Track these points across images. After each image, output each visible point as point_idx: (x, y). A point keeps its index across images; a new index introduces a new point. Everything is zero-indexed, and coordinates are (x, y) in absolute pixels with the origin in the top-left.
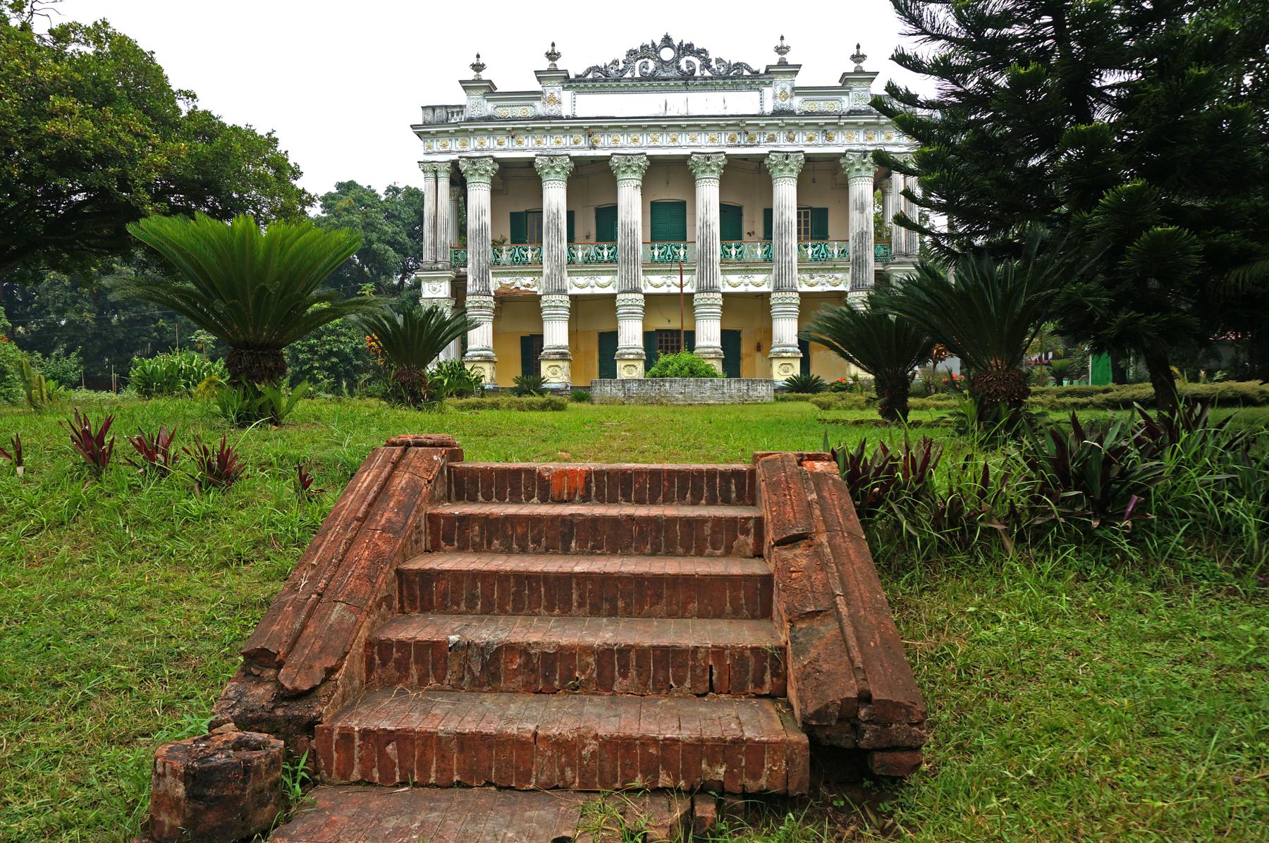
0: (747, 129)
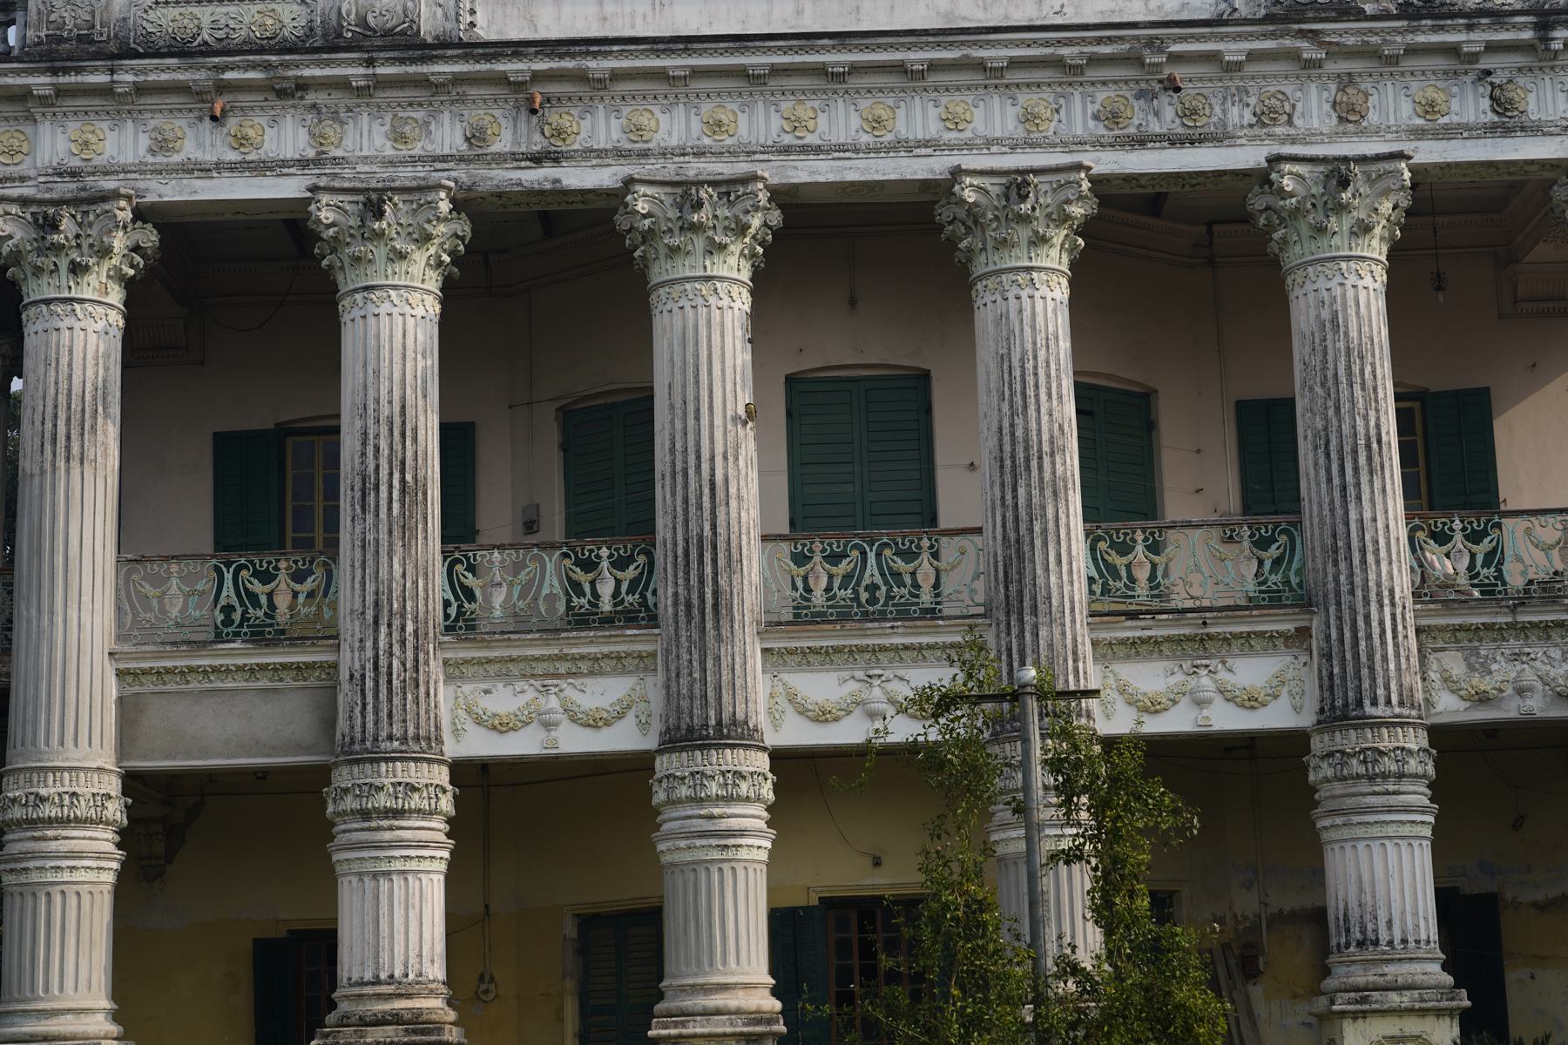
0: (1179, 72)
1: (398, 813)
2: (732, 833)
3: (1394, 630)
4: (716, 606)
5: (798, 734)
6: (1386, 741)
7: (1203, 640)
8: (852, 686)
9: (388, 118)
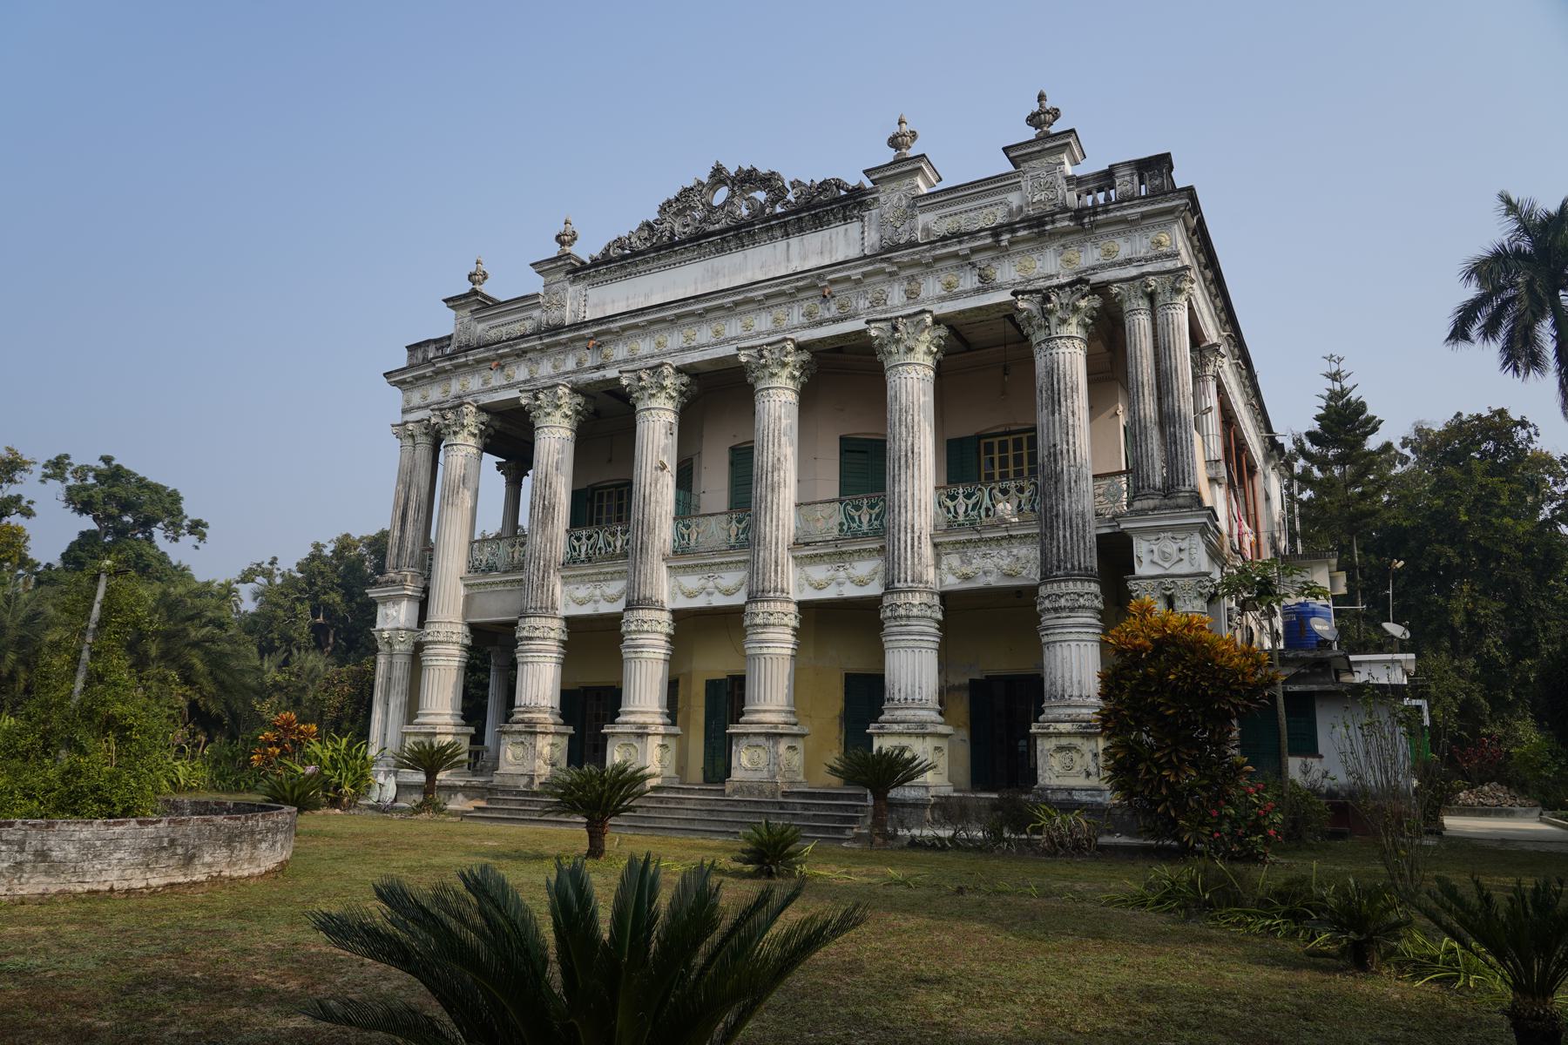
1: (531, 638)
2: (638, 646)
3: (913, 545)
4: (641, 549)
5: (683, 603)
6: (902, 599)
8: (703, 581)
9: (552, 360)
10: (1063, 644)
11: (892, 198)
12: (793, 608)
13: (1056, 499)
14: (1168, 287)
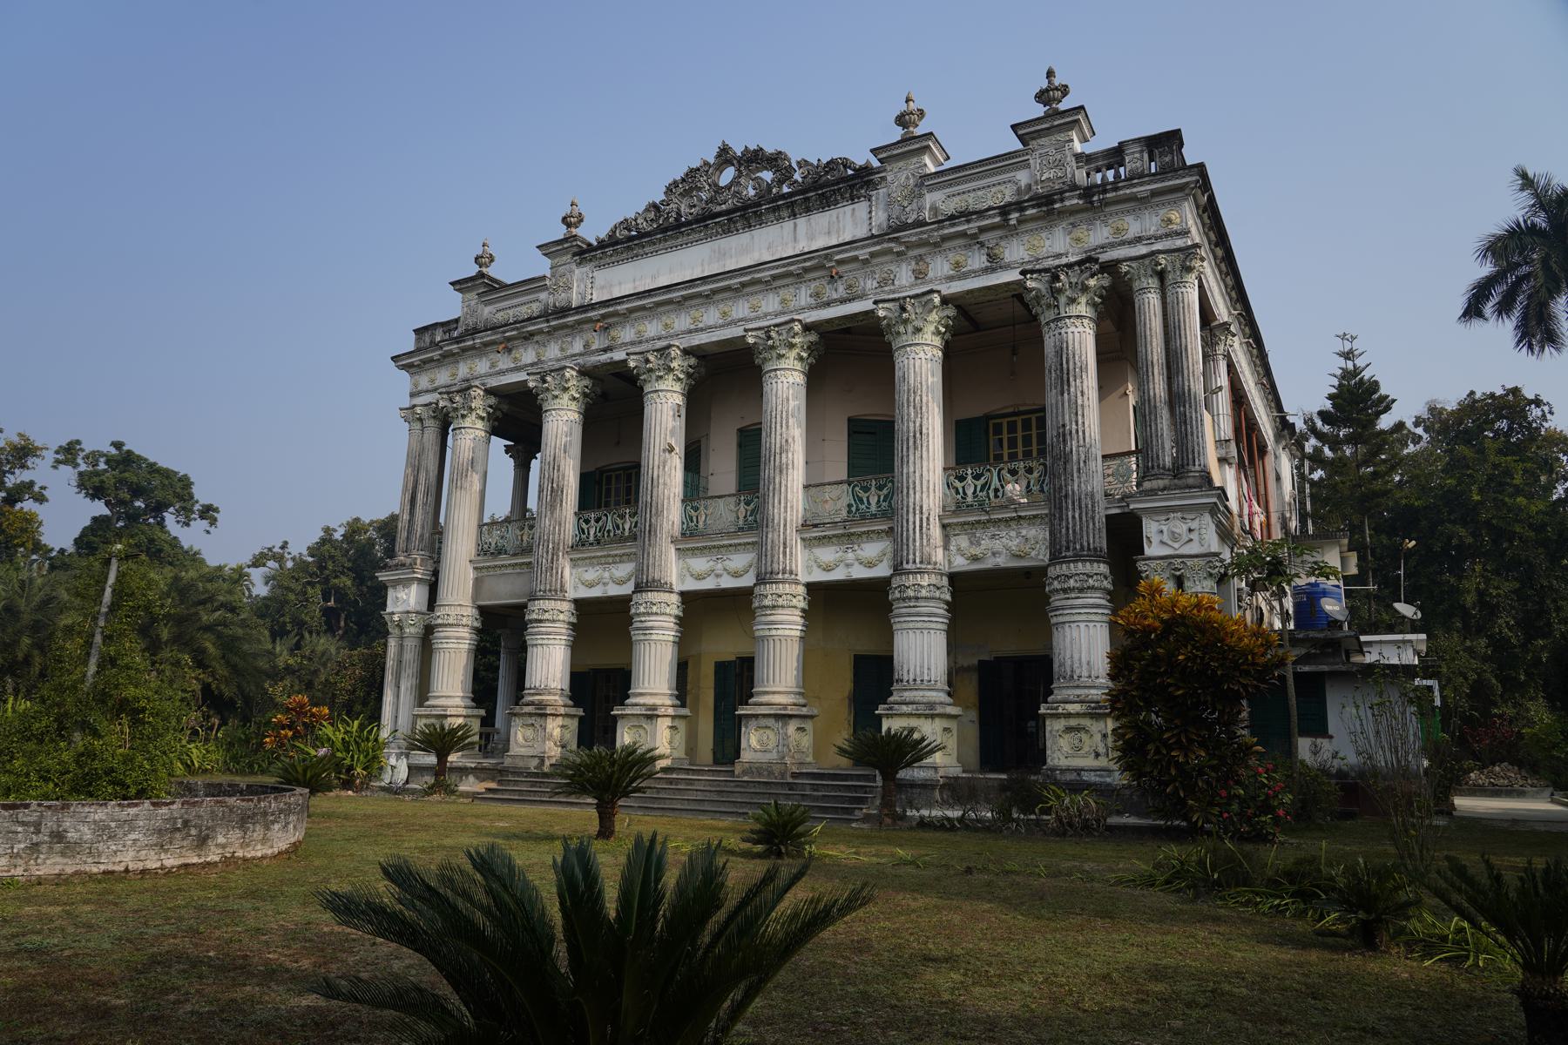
1: (540, 621)
2: (647, 628)
3: (921, 527)
4: (650, 531)
5: (692, 585)
6: (911, 580)
7: (850, 535)
8: (711, 563)
10: (1072, 625)
11: (899, 177)
12: (801, 590)
13: (1065, 480)
14: (1178, 265)
